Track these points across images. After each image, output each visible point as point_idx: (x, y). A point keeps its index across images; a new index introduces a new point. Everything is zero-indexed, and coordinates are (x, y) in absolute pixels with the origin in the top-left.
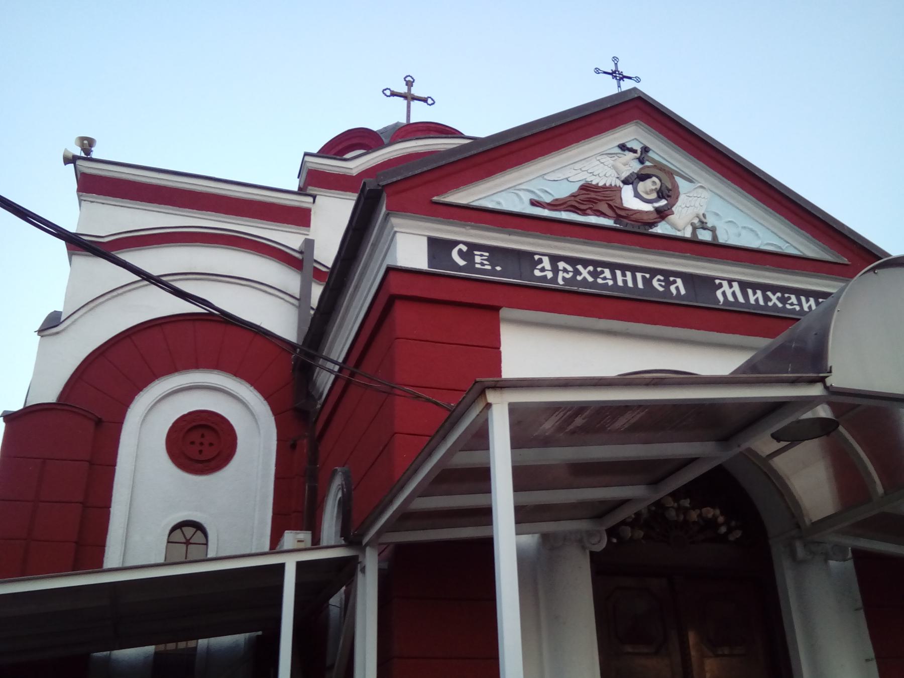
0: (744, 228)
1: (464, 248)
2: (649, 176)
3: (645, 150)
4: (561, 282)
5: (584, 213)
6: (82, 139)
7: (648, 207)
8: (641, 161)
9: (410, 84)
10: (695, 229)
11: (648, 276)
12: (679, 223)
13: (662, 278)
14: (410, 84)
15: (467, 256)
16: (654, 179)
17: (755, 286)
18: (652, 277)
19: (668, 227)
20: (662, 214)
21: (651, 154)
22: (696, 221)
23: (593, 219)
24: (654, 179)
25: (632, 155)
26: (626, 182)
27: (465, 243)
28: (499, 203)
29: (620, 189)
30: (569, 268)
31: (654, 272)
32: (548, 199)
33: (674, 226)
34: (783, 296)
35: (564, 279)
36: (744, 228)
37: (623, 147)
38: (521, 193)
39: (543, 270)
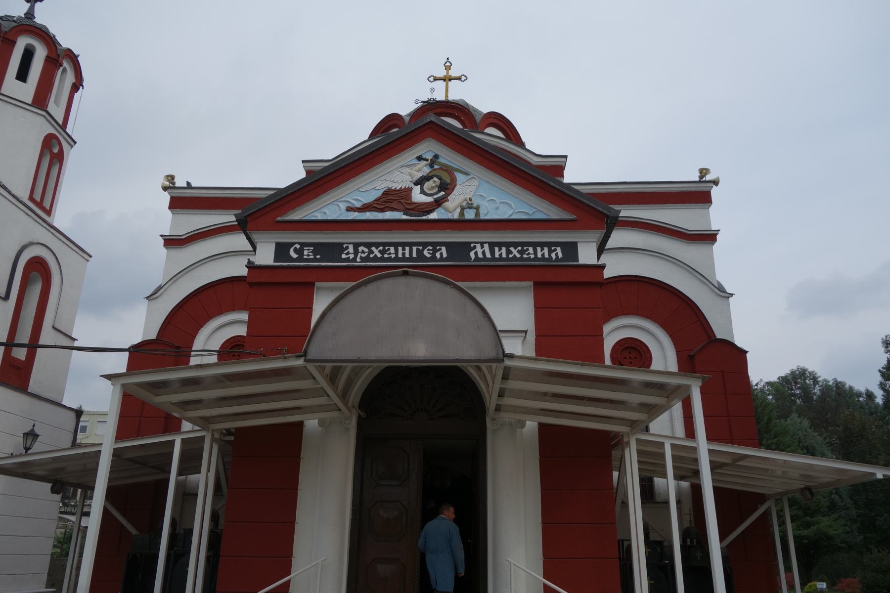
1: (298, 246)
2: (432, 178)
3: (436, 157)
4: (358, 260)
5: (382, 210)
6: (167, 176)
9: (448, 68)
10: (463, 209)
11: (421, 248)
12: (451, 209)
13: (431, 248)
14: (448, 68)
15: (299, 252)
16: (435, 179)
17: (500, 245)
19: (443, 211)
20: (438, 203)
21: (441, 160)
22: (464, 204)
23: (388, 215)
24: (435, 179)
25: (425, 162)
26: (416, 184)
27: (298, 243)
28: (325, 213)
29: (410, 190)
30: (366, 250)
31: (425, 245)
32: (358, 205)
33: (446, 210)
34: (522, 249)
35: (361, 257)
37: (420, 158)
38: (340, 204)
39: (348, 253)
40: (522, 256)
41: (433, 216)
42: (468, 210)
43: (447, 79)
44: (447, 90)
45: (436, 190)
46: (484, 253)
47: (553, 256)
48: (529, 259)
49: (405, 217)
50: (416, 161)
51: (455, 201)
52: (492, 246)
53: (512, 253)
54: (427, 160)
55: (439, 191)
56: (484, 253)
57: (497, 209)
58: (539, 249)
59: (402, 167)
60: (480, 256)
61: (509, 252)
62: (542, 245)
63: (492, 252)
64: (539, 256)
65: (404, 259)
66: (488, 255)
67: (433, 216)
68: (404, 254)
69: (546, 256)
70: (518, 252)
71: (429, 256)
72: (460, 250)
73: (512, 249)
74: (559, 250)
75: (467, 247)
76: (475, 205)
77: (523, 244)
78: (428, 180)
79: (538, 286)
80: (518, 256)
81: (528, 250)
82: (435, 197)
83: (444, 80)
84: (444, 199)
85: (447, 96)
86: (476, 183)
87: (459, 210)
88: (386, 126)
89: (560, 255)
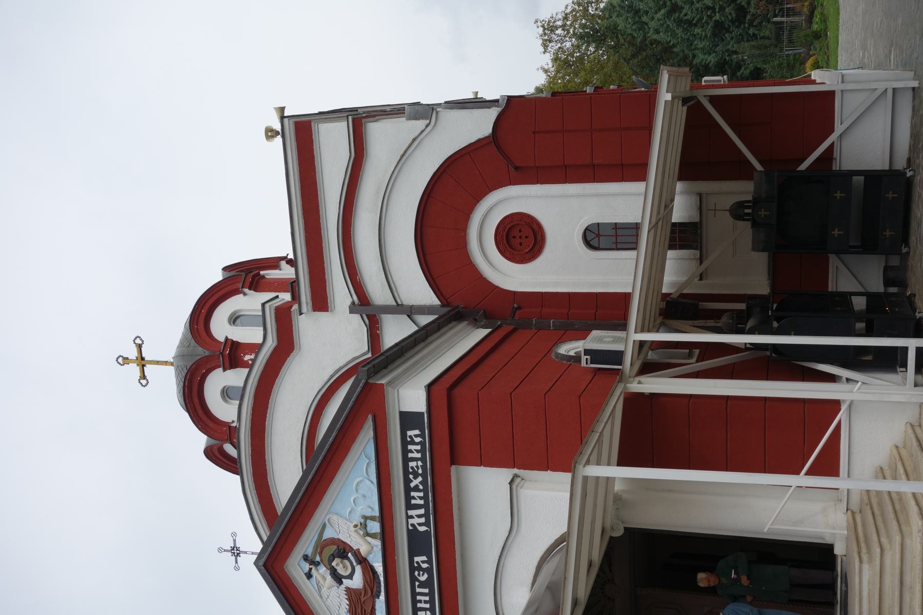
0: (357, 490)
3: (306, 558)
7: (358, 569)
8: (317, 564)
9: (126, 360)
10: (368, 534)
11: (417, 583)
13: (416, 573)
14: (126, 360)
16: (334, 564)
17: (408, 498)
18: (418, 581)
20: (363, 561)
21: (309, 552)
22: (362, 533)
24: (334, 564)
25: (313, 571)
26: (341, 583)
29: (348, 590)
31: (413, 579)
33: (370, 553)
34: (411, 473)
36: (357, 490)
37: (309, 576)
40: (420, 475)
41: (379, 568)
42: (369, 529)
43: (142, 361)
44: (157, 363)
45: (346, 562)
46: (419, 516)
47: (418, 440)
48: (424, 467)
49: (382, 597)
50: (313, 580)
51: (356, 541)
52: (409, 506)
53: (417, 486)
54: (311, 569)
55: (348, 559)
56: (419, 516)
57: (364, 496)
58: (410, 455)
59: (321, 596)
60: (423, 520)
61: (416, 489)
62: (405, 451)
63: (417, 507)
64: (419, 455)
65: (431, 601)
66: (422, 511)
67: (379, 567)
68: (426, 602)
69: (418, 447)
70: (415, 478)
71: (426, 576)
72: (417, 542)
73: (412, 485)
74: (410, 433)
75: (413, 534)
76: (362, 521)
77: (406, 472)
78: (336, 570)
79: (455, 459)
80: (420, 479)
81: (412, 468)
82: (355, 564)
83: (143, 366)
84: (357, 554)
85: (166, 363)
86: (334, 518)
87: (369, 539)
88: (221, 457)
89: (417, 432)
